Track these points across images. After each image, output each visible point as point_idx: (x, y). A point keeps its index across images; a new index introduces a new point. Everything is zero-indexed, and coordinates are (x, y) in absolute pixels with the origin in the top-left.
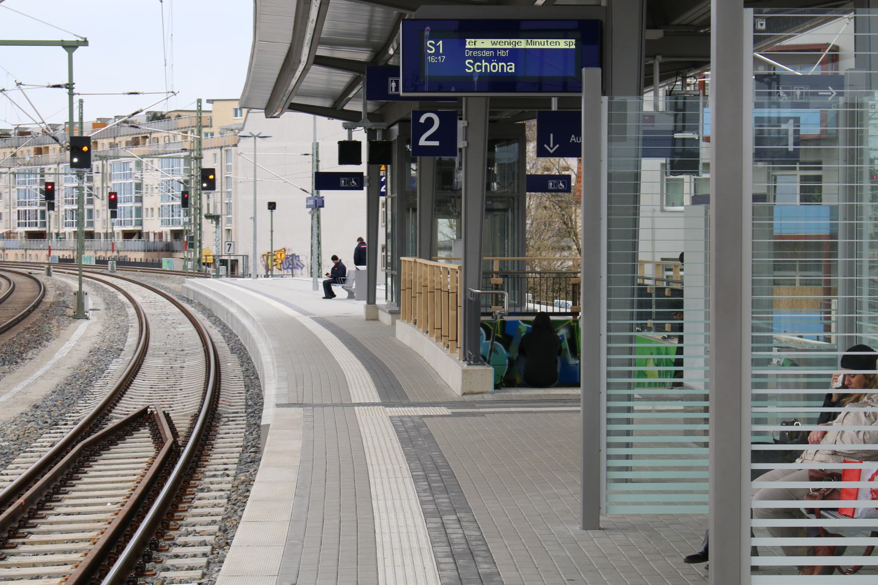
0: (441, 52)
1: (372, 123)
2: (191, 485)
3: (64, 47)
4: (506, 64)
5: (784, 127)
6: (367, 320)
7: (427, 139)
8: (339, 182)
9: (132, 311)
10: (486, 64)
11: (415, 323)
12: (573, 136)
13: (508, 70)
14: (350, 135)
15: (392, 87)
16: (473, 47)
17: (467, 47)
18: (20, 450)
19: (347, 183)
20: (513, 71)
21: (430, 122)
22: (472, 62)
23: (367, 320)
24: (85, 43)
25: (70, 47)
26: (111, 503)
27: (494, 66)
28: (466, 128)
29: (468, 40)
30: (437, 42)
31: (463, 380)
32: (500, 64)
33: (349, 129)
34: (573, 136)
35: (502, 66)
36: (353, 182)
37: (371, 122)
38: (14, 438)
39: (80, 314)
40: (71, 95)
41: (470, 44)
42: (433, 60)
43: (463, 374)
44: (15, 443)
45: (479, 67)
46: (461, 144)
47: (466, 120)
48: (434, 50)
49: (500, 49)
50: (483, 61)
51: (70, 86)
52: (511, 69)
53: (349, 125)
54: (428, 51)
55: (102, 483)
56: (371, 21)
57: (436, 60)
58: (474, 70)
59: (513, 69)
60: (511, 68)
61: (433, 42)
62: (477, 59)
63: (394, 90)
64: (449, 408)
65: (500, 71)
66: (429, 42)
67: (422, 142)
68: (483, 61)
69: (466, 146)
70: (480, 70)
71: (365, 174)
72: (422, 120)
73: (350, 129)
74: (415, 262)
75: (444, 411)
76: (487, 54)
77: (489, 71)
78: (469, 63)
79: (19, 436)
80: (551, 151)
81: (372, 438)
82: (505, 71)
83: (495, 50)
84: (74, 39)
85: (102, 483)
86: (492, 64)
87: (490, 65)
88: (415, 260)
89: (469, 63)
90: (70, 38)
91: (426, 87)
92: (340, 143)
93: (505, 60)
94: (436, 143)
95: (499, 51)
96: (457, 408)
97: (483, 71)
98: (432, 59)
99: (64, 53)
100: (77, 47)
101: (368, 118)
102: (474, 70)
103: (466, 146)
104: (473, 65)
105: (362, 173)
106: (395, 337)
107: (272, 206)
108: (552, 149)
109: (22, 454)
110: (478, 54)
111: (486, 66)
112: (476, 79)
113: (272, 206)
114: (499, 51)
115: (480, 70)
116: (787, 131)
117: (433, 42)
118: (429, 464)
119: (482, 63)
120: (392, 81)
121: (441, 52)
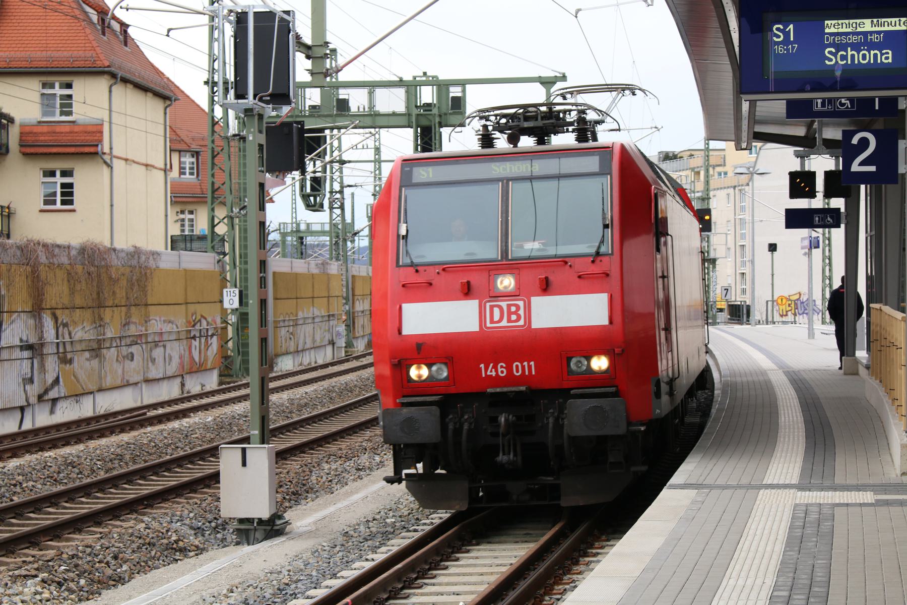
0: (792, 39)
1: (828, 150)
2: (564, 582)
3: (542, 83)
4: (881, 52)
6: (845, 374)
7: (862, 164)
8: (812, 220)
10: (853, 52)
11: (881, 382)
13: (883, 60)
14: (803, 165)
16: (836, 31)
17: (827, 31)
18: (405, 528)
19: (822, 220)
20: (890, 61)
21: (864, 143)
22: (834, 50)
23: (845, 374)
26: (464, 602)
27: (864, 56)
29: (826, 22)
30: (786, 27)
31: (901, 456)
32: (872, 52)
33: (801, 157)
35: (875, 55)
36: (829, 219)
37: (827, 148)
38: (406, 513)
41: (832, 26)
42: (781, 51)
44: (403, 519)
45: (844, 58)
48: (782, 37)
49: (871, 33)
50: (849, 49)
52: (887, 58)
53: (801, 153)
54: (775, 39)
55: (464, 575)
57: (785, 50)
58: (837, 62)
59: (890, 58)
60: (887, 57)
61: (781, 27)
62: (839, 47)
63: (819, 105)
64: (876, 492)
65: (872, 62)
66: (776, 27)
67: (855, 167)
68: (849, 49)
70: (845, 62)
71: (843, 210)
72: (855, 141)
73: (802, 156)
74: (881, 310)
75: (868, 497)
76: (854, 39)
77: (856, 62)
78: (830, 52)
79: (412, 510)
81: (755, 535)
82: (879, 61)
83: (865, 34)
84: (552, 74)
85: (464, 575)
86: (861, 53)
87: (858, 54)
88: (880, 307)
89: (830, 52)
90: (548, 73)
91: (772, 88)
92: (791, 174)
93: (880, 46)
94: (873, 169)
95: (871, 35)
96: (886, 494)
97: (849, 62)
98: (780, 50)
100: (555, 83)
101: (824, 144)
102: (837, 62)
104: (835, 55)
105: (839, 209)
107: (773, 248)
109: (403, 534)
110: (841, 40)
111: (853, 56)
112: (838, 73)
113: (773, 248)
114: (871, 35)
115: (845, 62)
117: (781, 27)
118: (804, 579)
119: (847, 52)
121: (792, 39)
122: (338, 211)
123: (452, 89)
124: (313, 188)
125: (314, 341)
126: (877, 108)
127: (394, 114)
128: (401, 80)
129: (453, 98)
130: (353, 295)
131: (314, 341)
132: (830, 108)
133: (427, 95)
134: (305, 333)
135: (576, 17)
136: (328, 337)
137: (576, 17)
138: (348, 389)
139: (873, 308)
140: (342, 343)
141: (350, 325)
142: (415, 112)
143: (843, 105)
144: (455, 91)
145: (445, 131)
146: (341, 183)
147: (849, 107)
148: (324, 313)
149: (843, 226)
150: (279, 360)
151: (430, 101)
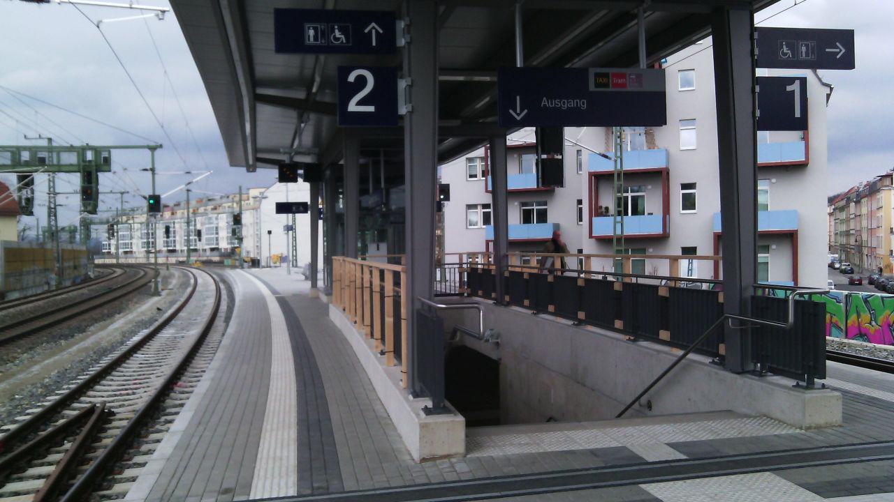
5: (789, 88)
7: (359, 103)
9: (189, 290)
12: (545, 99)
15: (309, 36)
21: (361, 81)
24: (161, 146)
25: (153, 149)
28: (410, 86)
34: (545, 99)
39: (157, 293)
40: (154, 174)
43: (421, 430)
46: (403, 110)
47: (410, 76)
51: (153, 170)
56: (302, 67)
63: (312, 39)
67: (353, 107)
69: (411, 110)
71: (309, 203)
80: (518, 118)
90: (152, 144)
94: (371, 109)
99: (148, 152)
103: (411, 110)
106: (328, 315)
107: (270, 232)
108: (518, 115)
113: (270, 232)
116: (793, 92)
120: (309, 28)
122: (53, 218)
123: (103, 153)
124: (26, 204)
125: (34, 282)
126: (374, 44)
127: (71, 165)
128: (72, 146)
129: (104, 158)
130: (62, 258)
131: (34, 282)
132: (323, 42)
133: (90, 156)
134: (28, 280)
135: (98, 27)
136: (44, 280)
137: (98, 27)
138: (21, 313)
139: (335, 259)
140: (53, 283)
141: (61, 274)
142: (82, 164)
143: (338, 39)
144: (105, 154)
145: (101, 175)
146: (55, 204)
147: (344, 41)
148: (41, 268)
149: (309, 212)
150: (8, 294)
151: (91, 159)
